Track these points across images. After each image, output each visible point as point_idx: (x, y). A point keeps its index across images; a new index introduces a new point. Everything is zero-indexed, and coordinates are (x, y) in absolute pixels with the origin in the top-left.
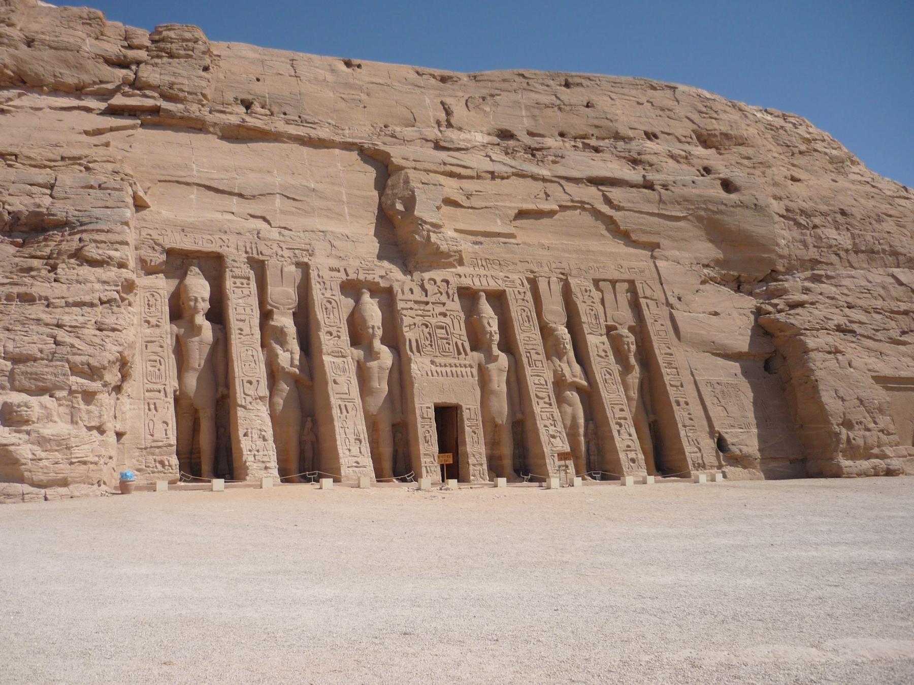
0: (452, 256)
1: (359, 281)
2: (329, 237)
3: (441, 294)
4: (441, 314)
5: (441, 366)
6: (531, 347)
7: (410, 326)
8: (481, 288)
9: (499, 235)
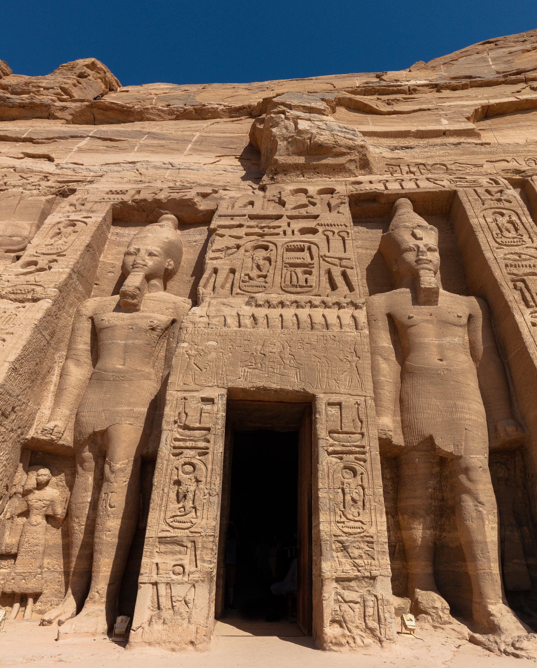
0: (343, 154)
1: (157, 202)
2: (138, 166)
3: (314, 204)
4: (304, 231)
5: (269, 304)
6: (528, 270)
7: (228, 248)
8: (403, 192)
9: (444, 133)
